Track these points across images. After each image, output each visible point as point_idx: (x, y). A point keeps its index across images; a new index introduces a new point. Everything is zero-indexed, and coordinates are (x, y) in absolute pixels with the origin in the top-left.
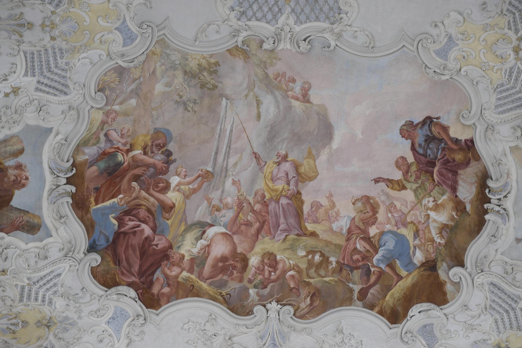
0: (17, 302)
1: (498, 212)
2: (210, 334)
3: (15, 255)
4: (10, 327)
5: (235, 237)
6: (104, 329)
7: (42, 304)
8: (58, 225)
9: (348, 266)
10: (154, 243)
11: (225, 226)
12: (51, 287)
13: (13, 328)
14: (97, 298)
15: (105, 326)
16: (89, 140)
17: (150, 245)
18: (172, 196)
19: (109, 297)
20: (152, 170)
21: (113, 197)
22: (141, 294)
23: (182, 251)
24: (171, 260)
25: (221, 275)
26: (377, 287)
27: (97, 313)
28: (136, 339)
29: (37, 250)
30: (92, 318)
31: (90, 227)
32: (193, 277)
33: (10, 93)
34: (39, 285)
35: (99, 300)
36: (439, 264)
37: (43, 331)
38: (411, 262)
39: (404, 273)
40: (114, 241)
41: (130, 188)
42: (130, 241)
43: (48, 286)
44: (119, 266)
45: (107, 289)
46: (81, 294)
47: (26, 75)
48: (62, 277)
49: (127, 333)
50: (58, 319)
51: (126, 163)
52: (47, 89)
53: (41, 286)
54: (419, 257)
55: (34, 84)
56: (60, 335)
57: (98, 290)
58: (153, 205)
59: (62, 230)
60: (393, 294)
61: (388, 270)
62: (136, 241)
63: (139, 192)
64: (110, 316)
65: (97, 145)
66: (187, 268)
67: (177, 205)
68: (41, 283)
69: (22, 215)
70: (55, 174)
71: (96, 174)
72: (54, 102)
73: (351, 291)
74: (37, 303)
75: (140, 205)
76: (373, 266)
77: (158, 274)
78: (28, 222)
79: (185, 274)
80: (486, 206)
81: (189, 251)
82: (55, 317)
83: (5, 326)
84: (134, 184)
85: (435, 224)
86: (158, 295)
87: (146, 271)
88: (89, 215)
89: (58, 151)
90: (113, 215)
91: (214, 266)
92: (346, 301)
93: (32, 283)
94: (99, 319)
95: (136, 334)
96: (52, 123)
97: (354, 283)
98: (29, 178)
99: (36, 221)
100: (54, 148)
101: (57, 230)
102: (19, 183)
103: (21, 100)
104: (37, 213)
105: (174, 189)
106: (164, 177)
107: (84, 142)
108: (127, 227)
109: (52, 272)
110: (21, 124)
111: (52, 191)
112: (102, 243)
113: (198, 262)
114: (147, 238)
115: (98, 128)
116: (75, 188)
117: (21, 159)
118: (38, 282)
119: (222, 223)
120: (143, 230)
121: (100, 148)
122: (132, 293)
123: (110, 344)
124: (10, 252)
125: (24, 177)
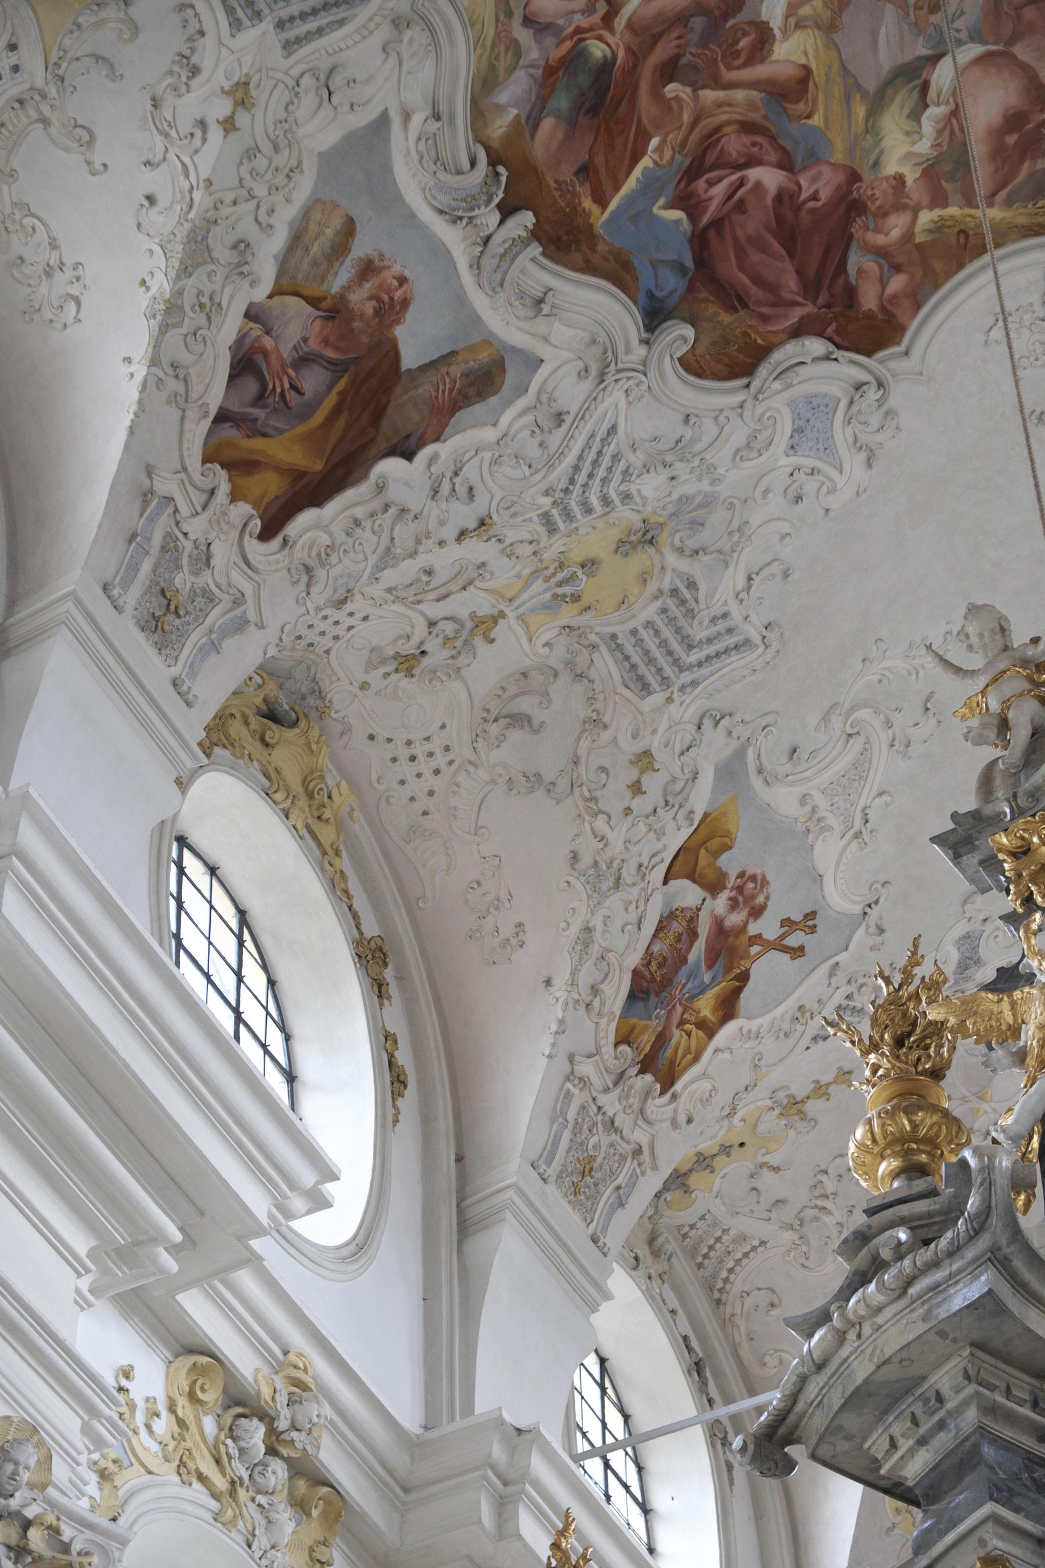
0: (544, 540)
3: (485, 468)
4: (560, 591)
5: (1021, 51)
6: (789, 470)
7: (607, 510)
8: (540, 325)
10: (804, 195)
11: (976, 37)
12: (609, 470)
13: (567, 590)
14: (733, 415)
15: (788, 462)
16: (492, 68)
17: (797, 209)
18: (790, 51)
19: (761, 397)
20: (698, 22)
21: (635, 159)
22: (838, 332)
23: (891, 167)
24: (872, 207)
25: (1027, 165)
27: (751, 446)
28: (880, 437)
29: (529, 418)
30: (747, 464)
31: (619, 272)
32: (953, 211)
33: (233, 113)
34: (578, 486)
35: (741, 415)
37: (642, 558)
40: (700, 262)
41: (668, 107)
42: (740, 233)
43: (601, 473)
44: (745, 306)
45: (745, 381)
46: (688, 434)
47: (236, 25)
48: (621, 429)
49: (851, 440)
50: (664, 513)
51: (621, 54)
52: (312, 25)
53: (585, 486)
55: (274, 40)
56: (692, 544)
57: (723, 396)
58: (751, 105)
59: (560, 332)
62: (753, 223)
63: (696, 98)
64: (788, 431)
65: (521, 62)
66: (925, 199)
67: (813, 65)
68: (582, 478)
69: (444, 370)
70: (461, 218)
71: (560, 134)
72: (350, 42)
74: (594, 516)
75: (717, 129)
77: (856, 260)
78: (467, 375)
79: (926, 217)
81: (909, 155)
82: (655, 513)
83: (548, 596)
84: (672, 89)
86: (883, 308)
87: (820, 275)
88: (601, 247)
89: (433, 153)
90: (661, 201)
91: (997, 152)
93: (562, 495)
94: (766, 455)
95: (876, 427)
96: (380, 96)
98: (407, 273)
99: (484, 356)
100: (422, 158)
101: (545, 339)
102: (392, 308)
103: (270, 103)
104: (476, 338)
105: (785, 31)
106: (742, 17)
107: (485, 81)
108: (713, 207)
109: (592, 436)
110: (305, 166)
111: (476, 265)
112: (672, 284)
113: (947, 167)
114: (779, 198)
115: (497, 20)
116: (530, 213)
117: (361, 248)
118: (572, 481)
119: (963, 35)
120: (758, 185)
121: (531, 66)
122: (816, 346)
123: (824, 489)
124: (470, 472)
125: (395, 283)
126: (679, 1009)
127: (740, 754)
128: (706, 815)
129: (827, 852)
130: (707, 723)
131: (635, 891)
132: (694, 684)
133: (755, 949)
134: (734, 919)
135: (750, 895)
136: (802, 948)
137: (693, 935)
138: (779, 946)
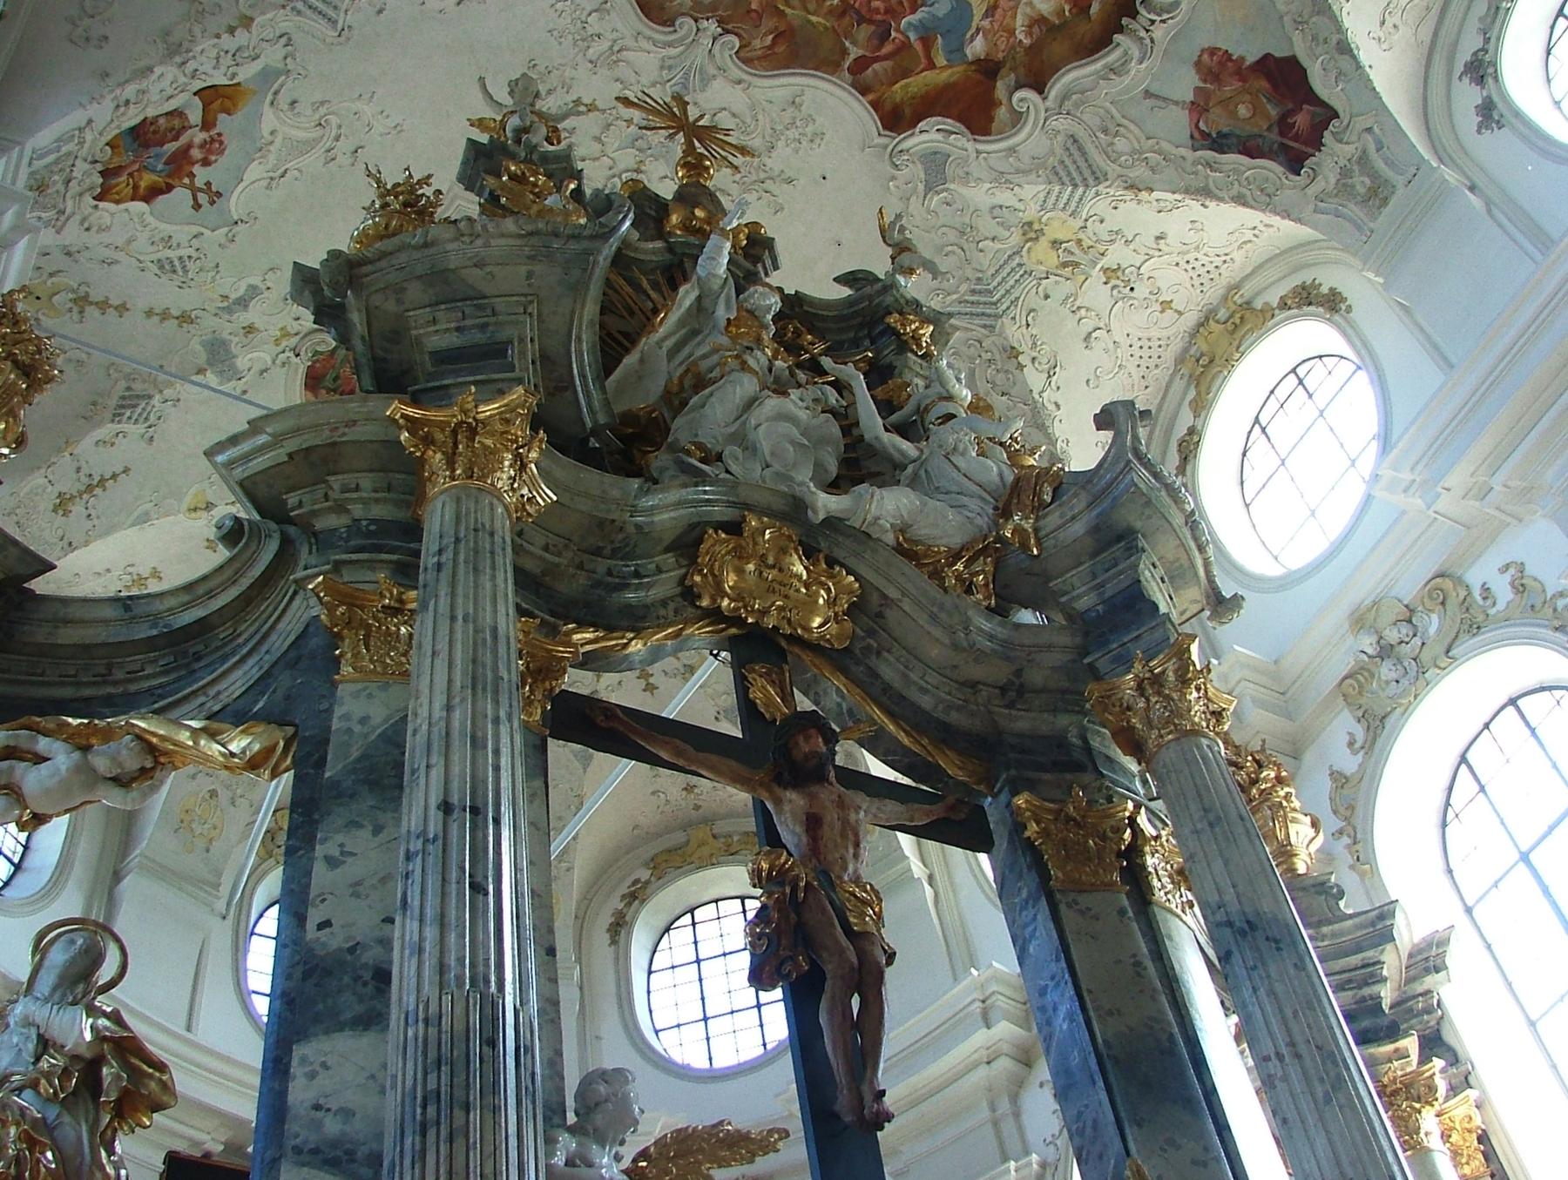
1: (1142, 38)
2: (590, 31)
9: (857, 12)
26: (888, 64)
36: (1003, 72)
38: (960, 49)
39: (941, 61)
54: (977, 47)
60: (907, 85)
61: (918, 46)
73: (844, 52)
76: (898, 30)
80: (1125, 21)
85: (1028, 10)
92: (827, 63)
97: (854, 43)
126: (136, 166)
127: (279, 73)
128: (239, 84)
129: (255, 172)
130: (283, 40)
131: (182, 79)
132: (299, 13)
133: (186, 180)
134: (196, 153)
135: (214, 147)
136: (200, 206)
137: (176, 138)
138: (195, 192)
